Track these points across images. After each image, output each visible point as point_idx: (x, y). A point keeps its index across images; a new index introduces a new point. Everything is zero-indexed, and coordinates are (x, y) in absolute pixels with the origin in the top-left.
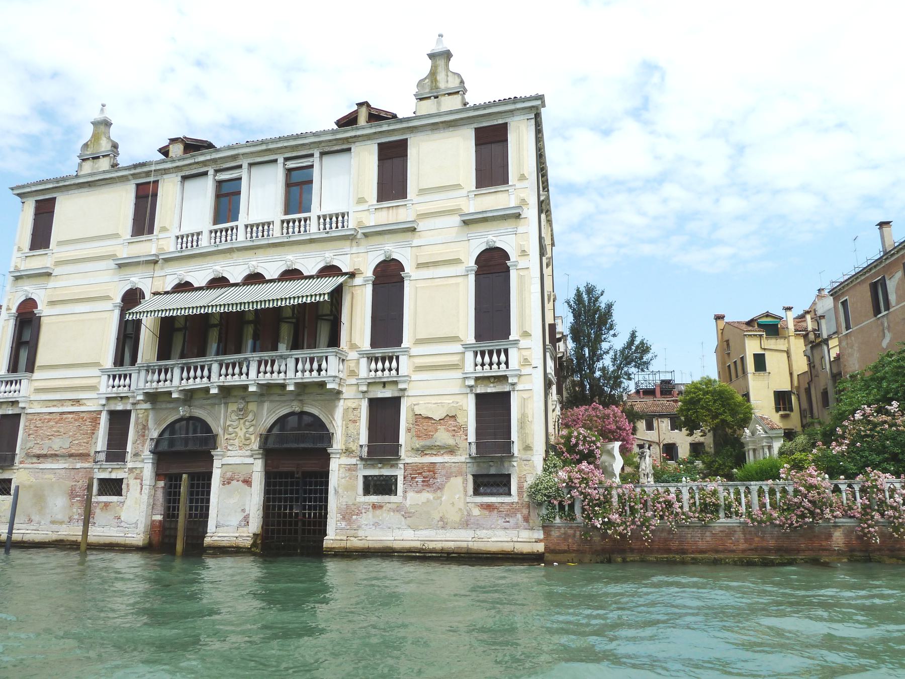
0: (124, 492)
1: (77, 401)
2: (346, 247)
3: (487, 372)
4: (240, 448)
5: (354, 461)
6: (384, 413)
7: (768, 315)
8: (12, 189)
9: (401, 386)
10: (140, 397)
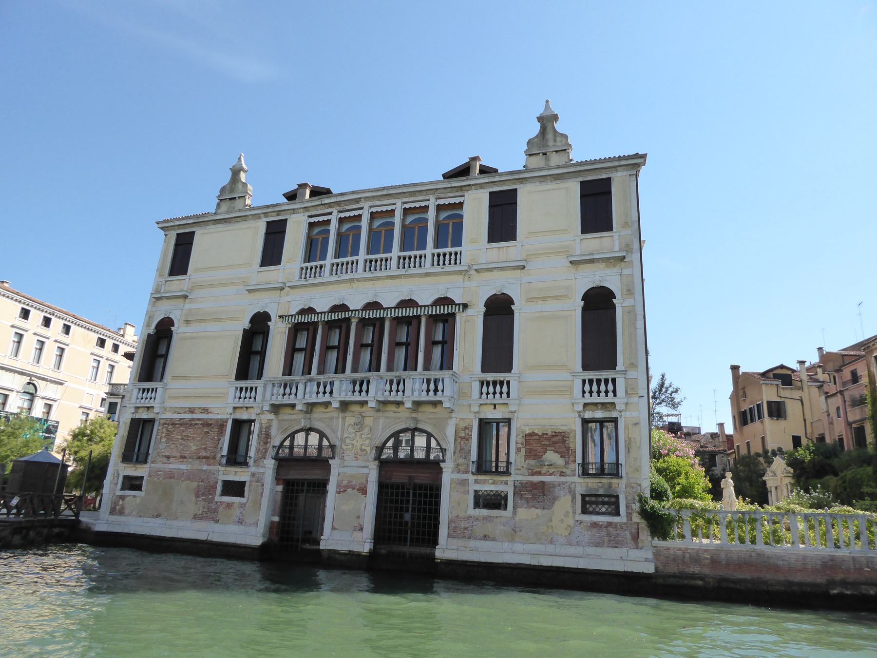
0: (246, 494)
1: (205, 410)
3: (595, 399)
7: (782, 367)
8: (158, 223)
9: (512, 408)
10: (267, 408)
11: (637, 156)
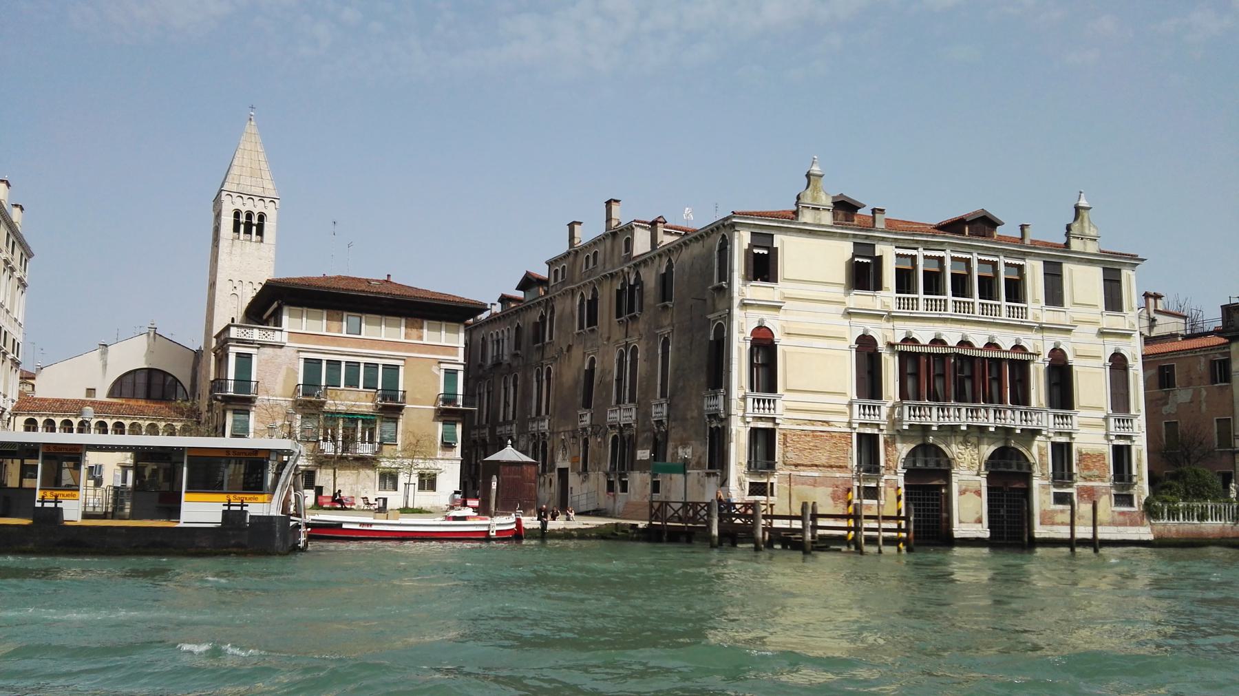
2: (1029, 334)
4: (969, 469)
5: (1046, 482)
6: (1062, 452)
11: (1133, 257)
